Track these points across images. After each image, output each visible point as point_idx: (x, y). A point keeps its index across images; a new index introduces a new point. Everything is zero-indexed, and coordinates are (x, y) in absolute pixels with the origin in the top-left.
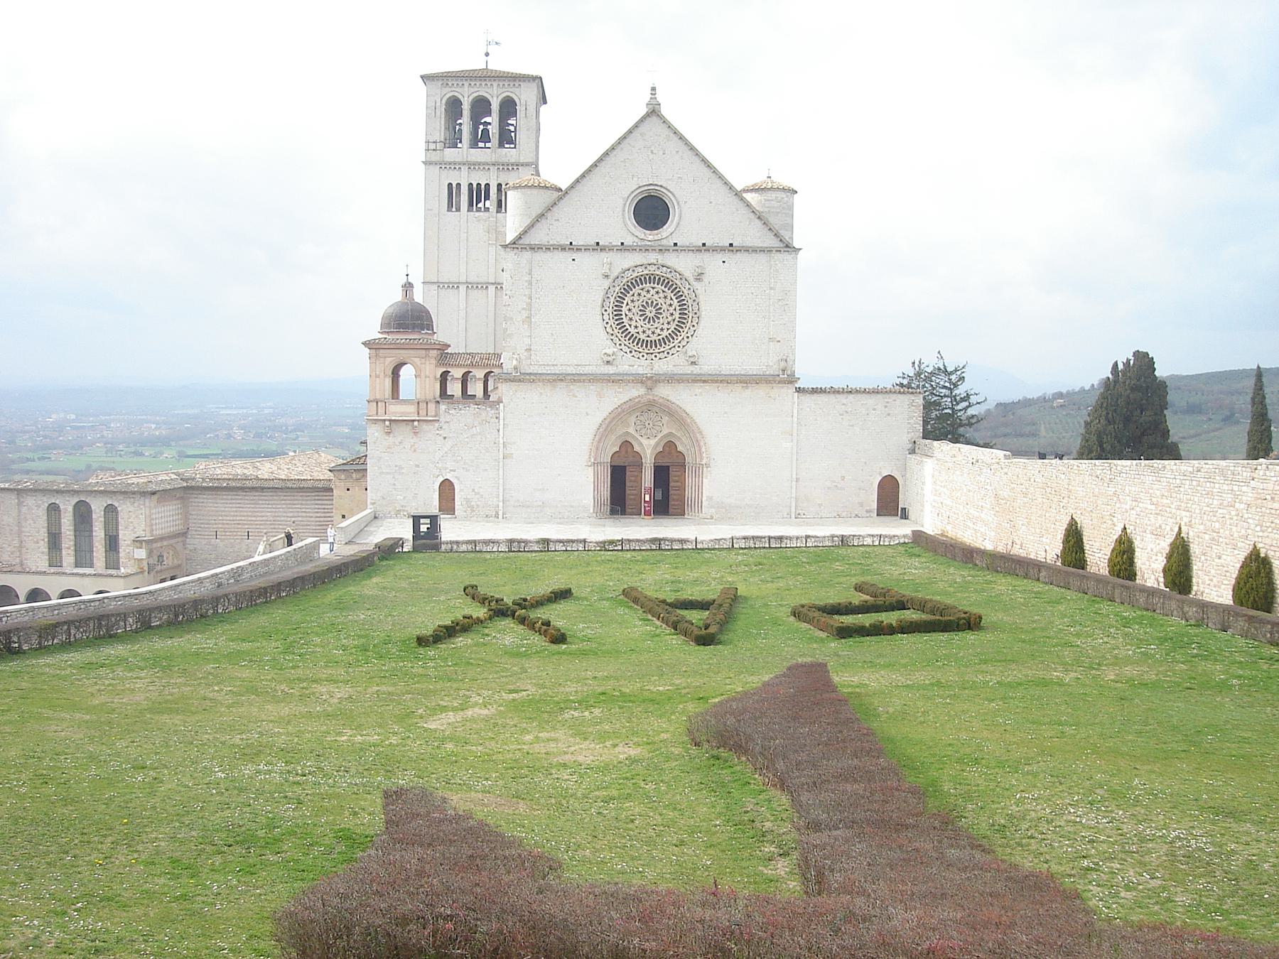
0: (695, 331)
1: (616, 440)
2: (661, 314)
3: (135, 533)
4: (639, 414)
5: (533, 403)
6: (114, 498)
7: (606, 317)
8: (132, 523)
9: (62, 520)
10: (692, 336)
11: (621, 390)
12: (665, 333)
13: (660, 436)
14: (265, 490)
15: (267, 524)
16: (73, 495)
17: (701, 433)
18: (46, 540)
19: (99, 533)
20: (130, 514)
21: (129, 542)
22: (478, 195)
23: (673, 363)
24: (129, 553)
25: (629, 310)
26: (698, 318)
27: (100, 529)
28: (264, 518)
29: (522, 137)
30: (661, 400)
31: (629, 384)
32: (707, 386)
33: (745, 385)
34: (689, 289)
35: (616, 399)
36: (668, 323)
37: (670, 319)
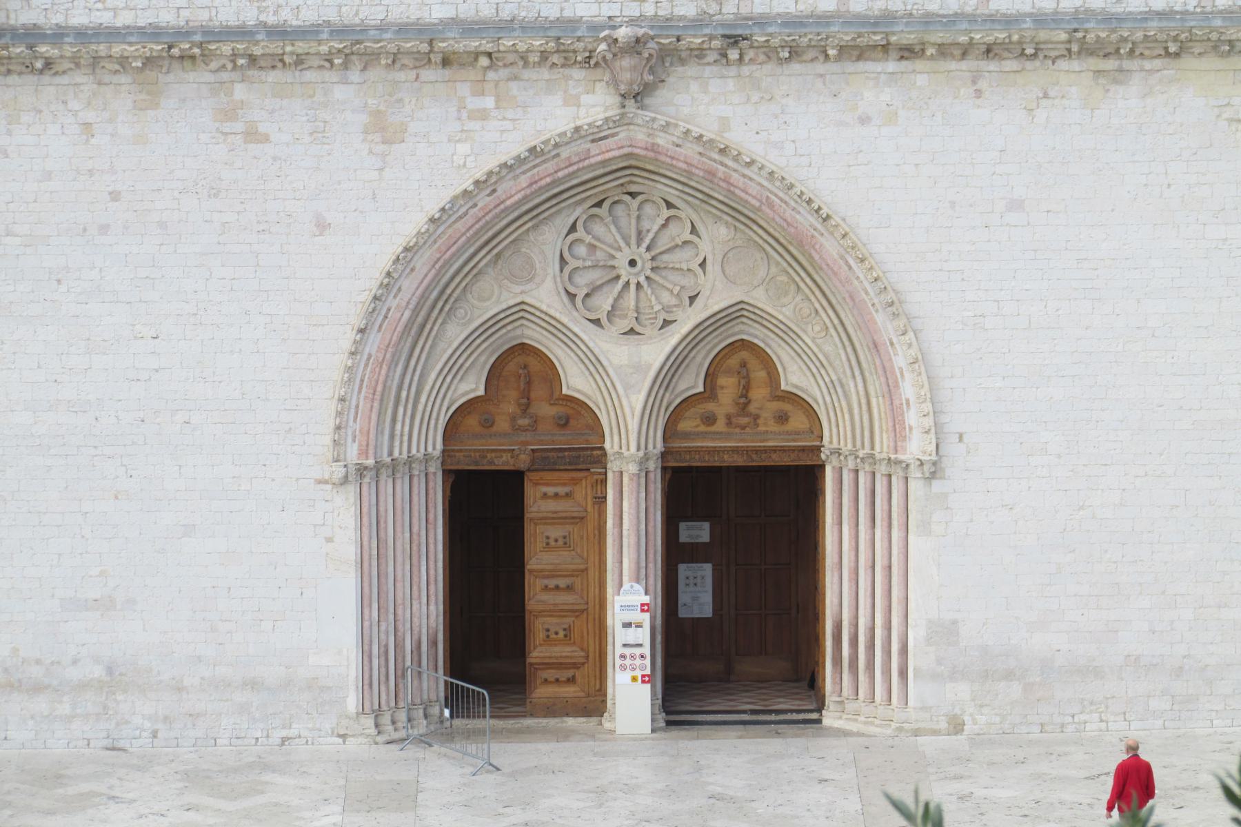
1: (469, 343)
5: (48, 176)
11: (489, 102)
13: (687, 321)
17: (894, 307)
30: (690, 151)
31: (527, 74)
32: (921, 75)
33: (1111, 64)
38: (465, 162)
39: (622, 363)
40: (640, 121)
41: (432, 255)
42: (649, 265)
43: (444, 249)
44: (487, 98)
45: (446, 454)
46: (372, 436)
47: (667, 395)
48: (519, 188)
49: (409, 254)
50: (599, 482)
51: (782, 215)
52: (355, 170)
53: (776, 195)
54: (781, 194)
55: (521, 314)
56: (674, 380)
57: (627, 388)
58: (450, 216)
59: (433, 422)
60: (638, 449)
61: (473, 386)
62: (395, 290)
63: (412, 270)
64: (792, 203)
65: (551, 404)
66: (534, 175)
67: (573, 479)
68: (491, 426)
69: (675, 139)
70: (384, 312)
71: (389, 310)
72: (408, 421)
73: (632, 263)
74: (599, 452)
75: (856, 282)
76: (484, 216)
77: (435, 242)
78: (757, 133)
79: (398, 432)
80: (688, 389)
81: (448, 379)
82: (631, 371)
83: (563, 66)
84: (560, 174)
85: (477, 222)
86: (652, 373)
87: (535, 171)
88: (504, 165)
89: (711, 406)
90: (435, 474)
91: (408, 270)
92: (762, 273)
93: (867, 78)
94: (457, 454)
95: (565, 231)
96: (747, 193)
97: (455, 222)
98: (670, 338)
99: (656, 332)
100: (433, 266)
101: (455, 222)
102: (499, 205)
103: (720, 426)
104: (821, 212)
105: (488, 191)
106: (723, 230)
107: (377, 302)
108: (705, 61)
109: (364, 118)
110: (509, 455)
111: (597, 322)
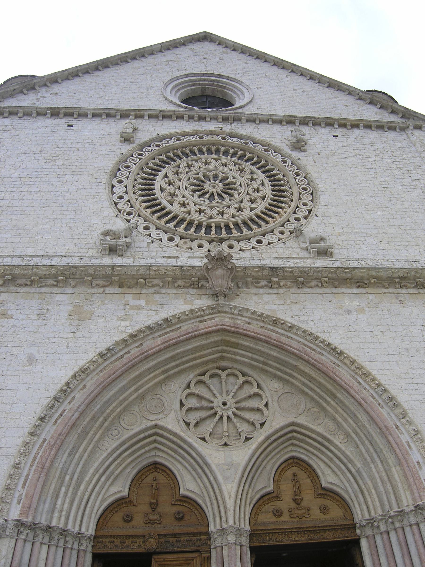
0: (310, 211)
2: (235, 189)
4: (191, 376)
7: (119, 190)
10: (306, 218)
11: (143, 302)
12: (247, 214)
23: (276, 255)
25: (170, 184)
26: (312, 194)
34: (284, 161)
35: (127, 323)
36: (252, 201)
37: (255, 195)
38: (125, 329)
39: (220, 463)
40: (227, 309)
41: (98, 379)
42: (234, 405)
43: (106, 376)
44: (142, 300)
45: (96, 540)
46: (35, 500)
47: (251, 490)
48: (156, 344)
49: (83, 374)
50: (206, 559)
51: (313, 357)
52: (59, 333)
53: (308, 347)
54: (311, 345)
55: (154, 437)
56: (254, 480)
57: (225, 478)
58: (113, 355)
59: (88, 509)
60: (235, 523)
61: (120, 489)
62: (70, 398)
63: (84, 387)
64: (318, 349)
65: (172, 505)
66: (165, 338)
67: (187, 559)
68: (130, 521)
69: (247, 319)
70: (60, 411)
71: (64, 411)
72: (68, 500)
73: (224, 404)
74: (205, 537)
75: (364, 391)
76: (134, 359)
77: (101, 371)
78: (292, 317)
79: (58, 506)
80: (263, 488)
81: (103, 479)
82: (227, 467)
83: (184, 287)
84: (181, 338)
85: (129, 362)
86: (241, 468)
87: (167, 336)
88: (149, 328)
89: (278, 504)
90: (85, 551)
91: (81, 386)
92: (302, 407)
93: (344, 296)
94: (104, 540)
95: (184, 386)
96: (291, 347)
97: (115, 361)
98: (251, 446)
99: (241, 444)
100: (98, 386)
101: (115, 361)
102: (143, 353)
103: (285, 517)
104: (337, 350)
105: (137, 344)
106: (276, 385)
107: (56, 402)
108: (260, 285)
109: (70, 308)
110: (142, 540)
111: (204, 439)
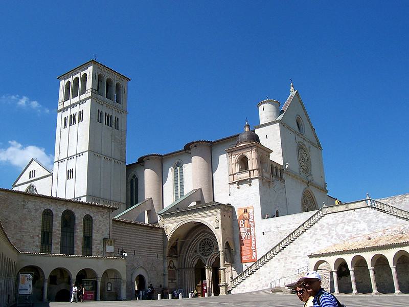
3: (103, 236)
6: (91, 210)
8: (101, 228)
9: (54, 222)
14: (126, 225)
15: (126, 245)
16: (63, 205)
18: (40, 236)
19: (79, 233)
20: (101, 222)
21: (99, 242)
22: (109, 118)
24: (98, 249)
27: (80, 231)
28: (126, 242)
29: (123, 100)
